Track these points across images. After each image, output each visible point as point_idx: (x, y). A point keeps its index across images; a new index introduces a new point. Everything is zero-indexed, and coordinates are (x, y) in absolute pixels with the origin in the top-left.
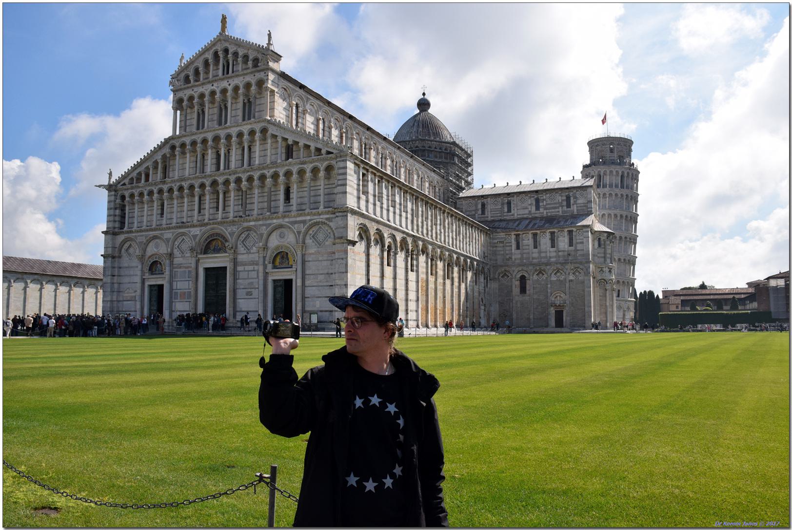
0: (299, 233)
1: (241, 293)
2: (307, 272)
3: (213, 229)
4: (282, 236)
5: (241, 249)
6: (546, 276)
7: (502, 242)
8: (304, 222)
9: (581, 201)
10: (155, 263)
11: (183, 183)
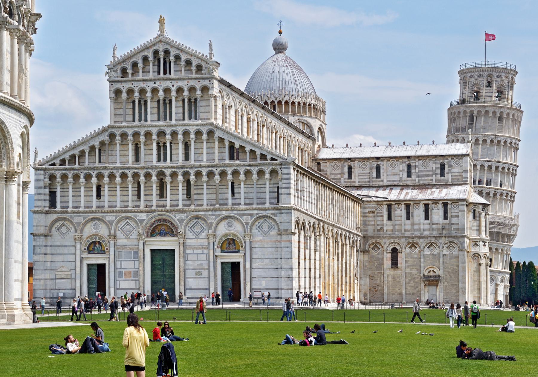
0: (247, 224)
2: (254, 256)
5: (189, 234)
6: (418, 249)
7: (373, 212)
8: (252, 215)
10: (94, 243)
11: (127, 171)
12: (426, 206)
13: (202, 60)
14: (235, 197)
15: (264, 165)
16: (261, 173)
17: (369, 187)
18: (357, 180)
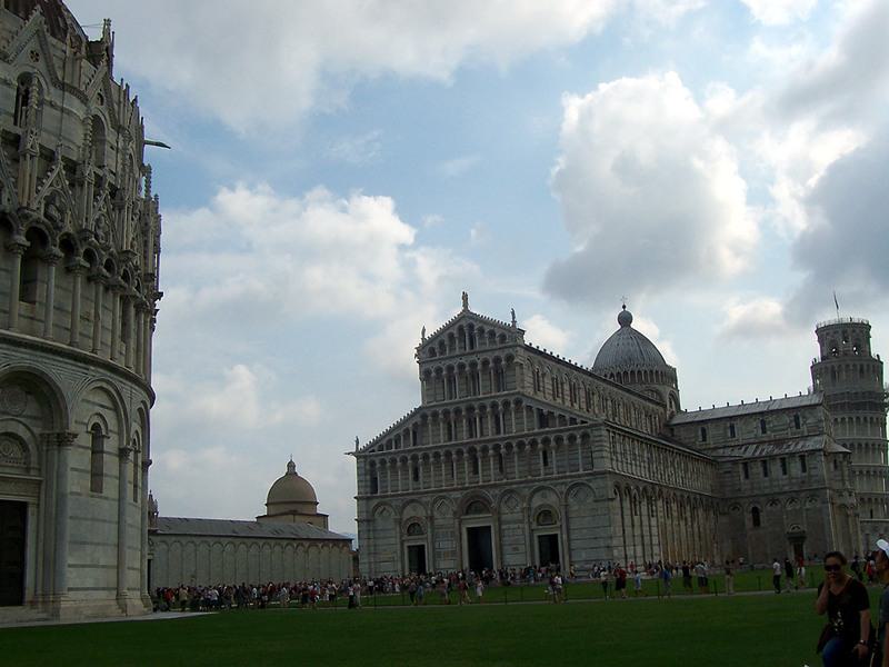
0: (561, 493)
1: (507, 549)
4: (544, 496)
5: (504, 509)
6: (779, 506)
10: (413, 525)
12: (783, 460)
15: (575, 429)
16: (572, 438)
17: (725, 447)
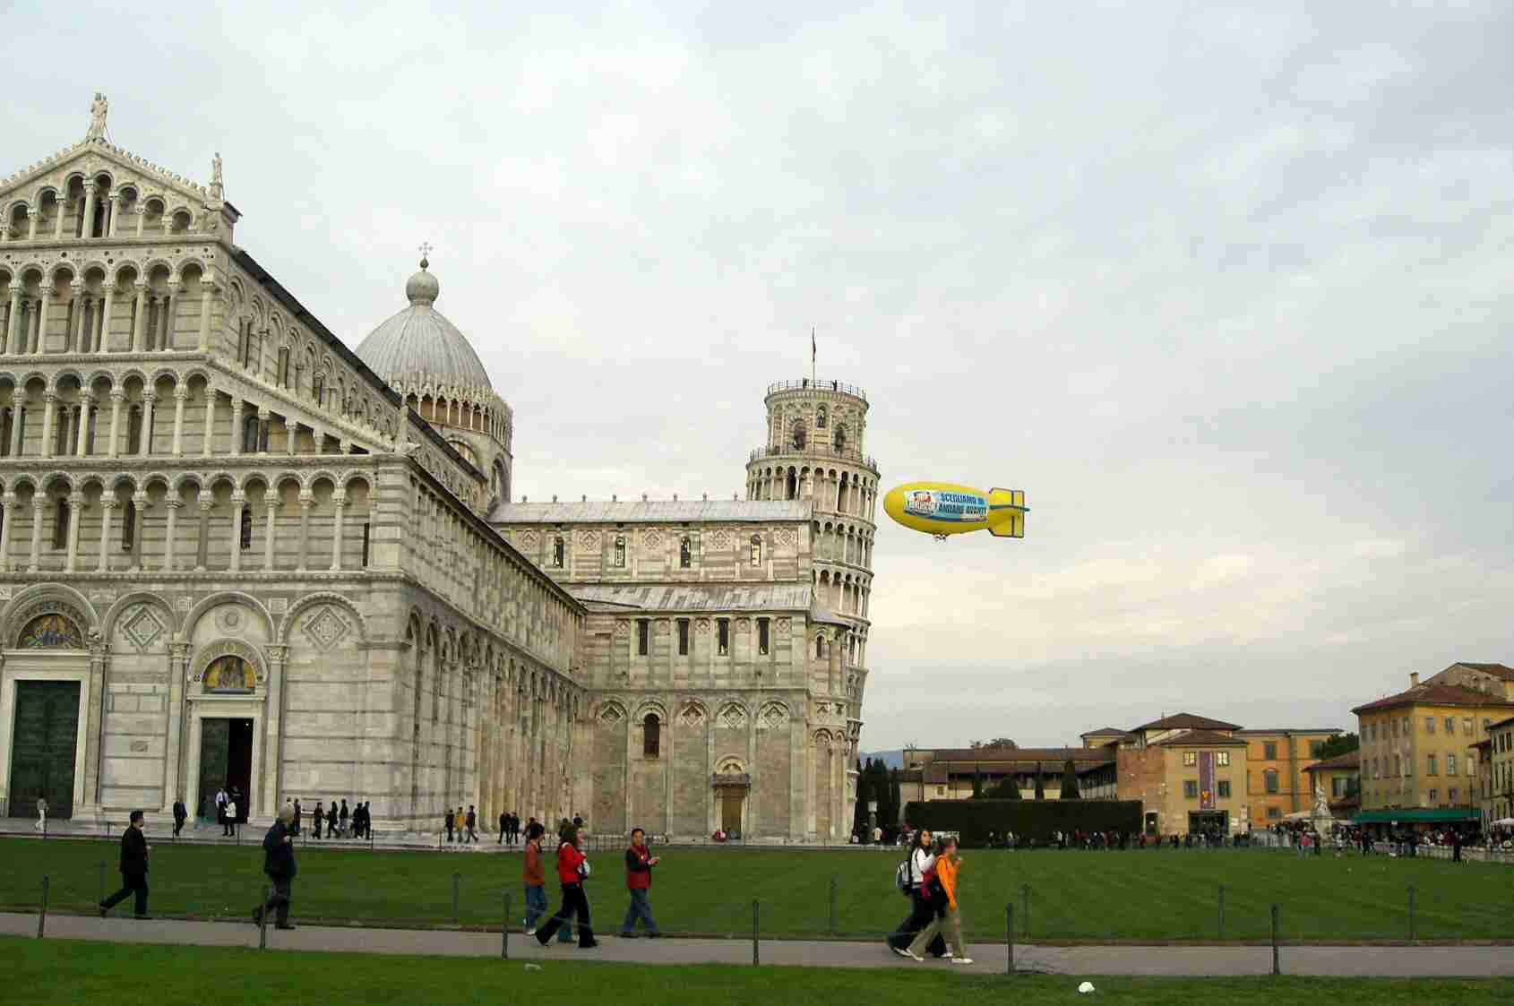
0: (277, 618)
1: (115, 745)
3: (44, 591)
5: (122, 643)
7: (608, 636)
8: (290, 596)
9: (783, 552)
12: (723, 623)
13: (191, 198)
14: (252, 550)
15: (332, 463)
16: (323, 484)
17: (600, 584)
18: (573, 570)
